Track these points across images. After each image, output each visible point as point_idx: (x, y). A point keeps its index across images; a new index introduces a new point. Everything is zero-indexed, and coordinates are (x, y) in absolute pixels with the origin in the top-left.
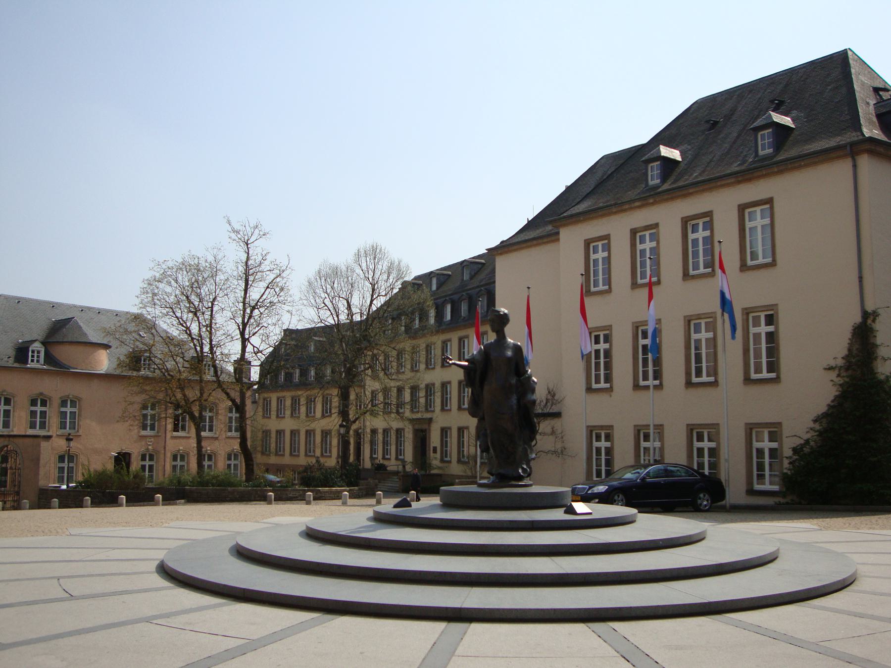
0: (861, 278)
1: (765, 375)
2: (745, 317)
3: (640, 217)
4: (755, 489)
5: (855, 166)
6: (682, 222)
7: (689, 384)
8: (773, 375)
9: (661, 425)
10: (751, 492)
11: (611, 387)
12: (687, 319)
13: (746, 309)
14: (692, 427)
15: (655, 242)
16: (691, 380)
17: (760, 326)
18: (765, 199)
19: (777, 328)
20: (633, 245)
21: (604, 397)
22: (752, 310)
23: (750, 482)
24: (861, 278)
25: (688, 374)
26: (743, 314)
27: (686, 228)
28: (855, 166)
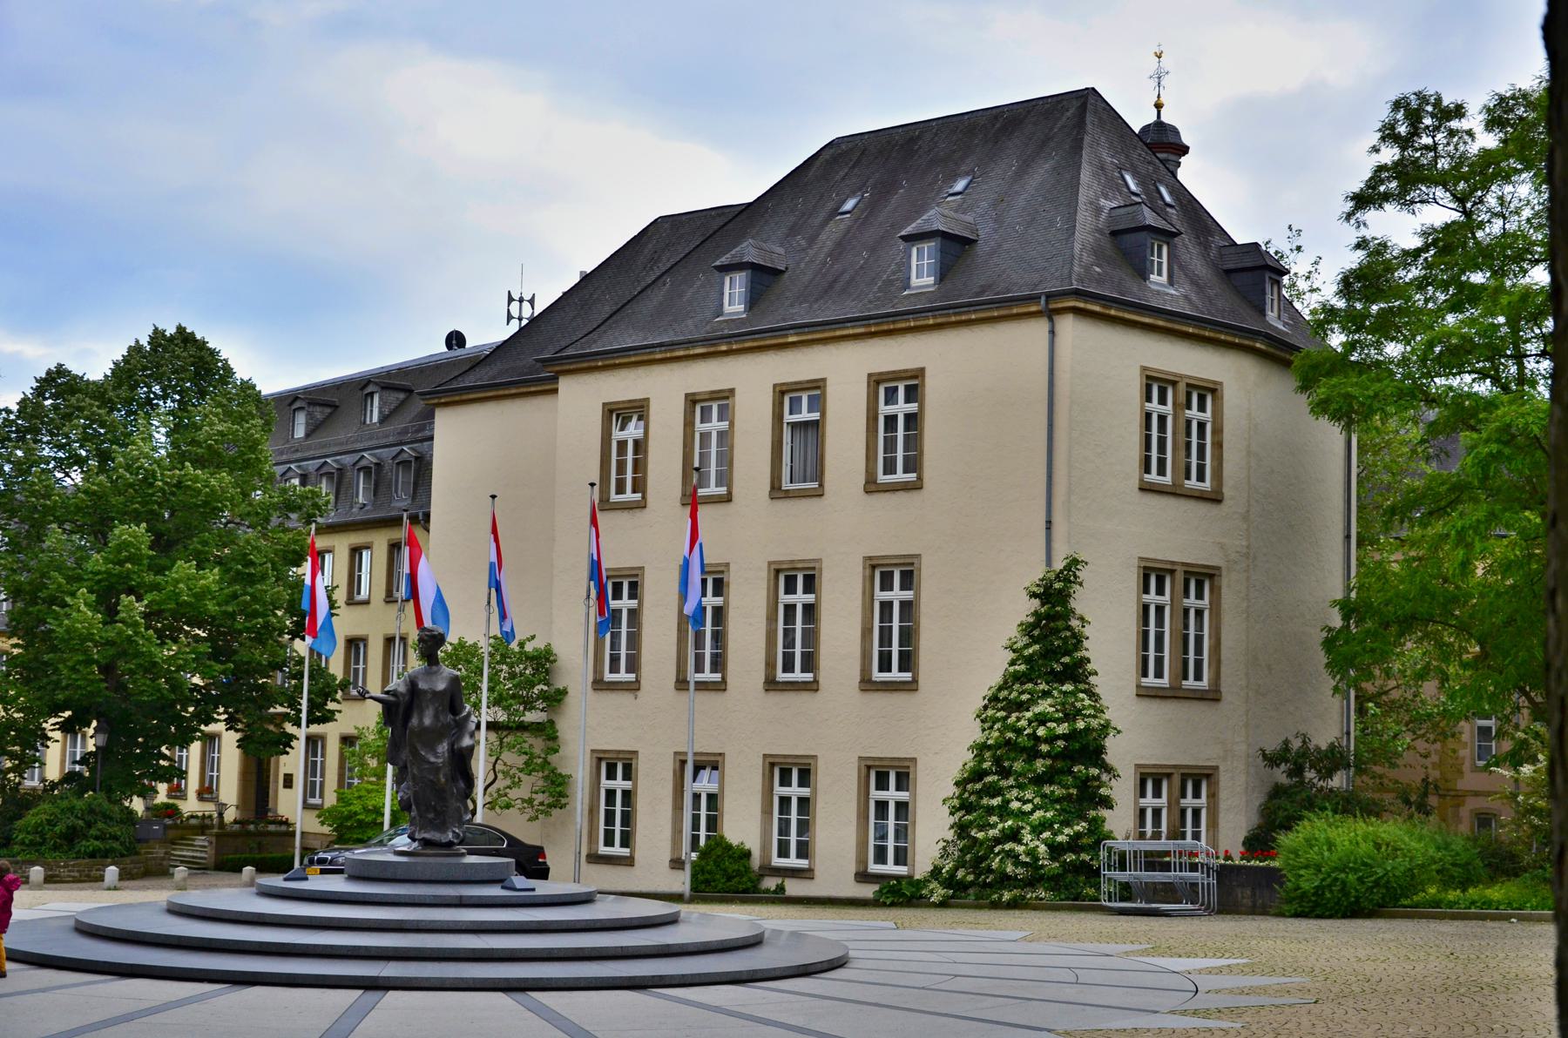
0: (1049, 523)
1: (895, 675)
2: (868, 572)
3: (705, 376)
4: (869, 870)
5: (1052, 332)
6: (774, 391)
7: (771, 684)
8: (907, 676)
9: (720, 754)
10: (863, 876)
11: (638, 681)
12: (773, 567)
13: (870, 558)
14: (772, 760)
15: (727, 423)
16: (775, 676)
17: (891, 589)
18: (912, 370)
19: (917, 595)
20: (689, 424)
21: (623, 699)
22: (881, 562)
23: (862, 860)
24: (1049, 523)
25: (770, 665)
26: (864, 568)
27: (782, 404)
28: (1052, 332)
